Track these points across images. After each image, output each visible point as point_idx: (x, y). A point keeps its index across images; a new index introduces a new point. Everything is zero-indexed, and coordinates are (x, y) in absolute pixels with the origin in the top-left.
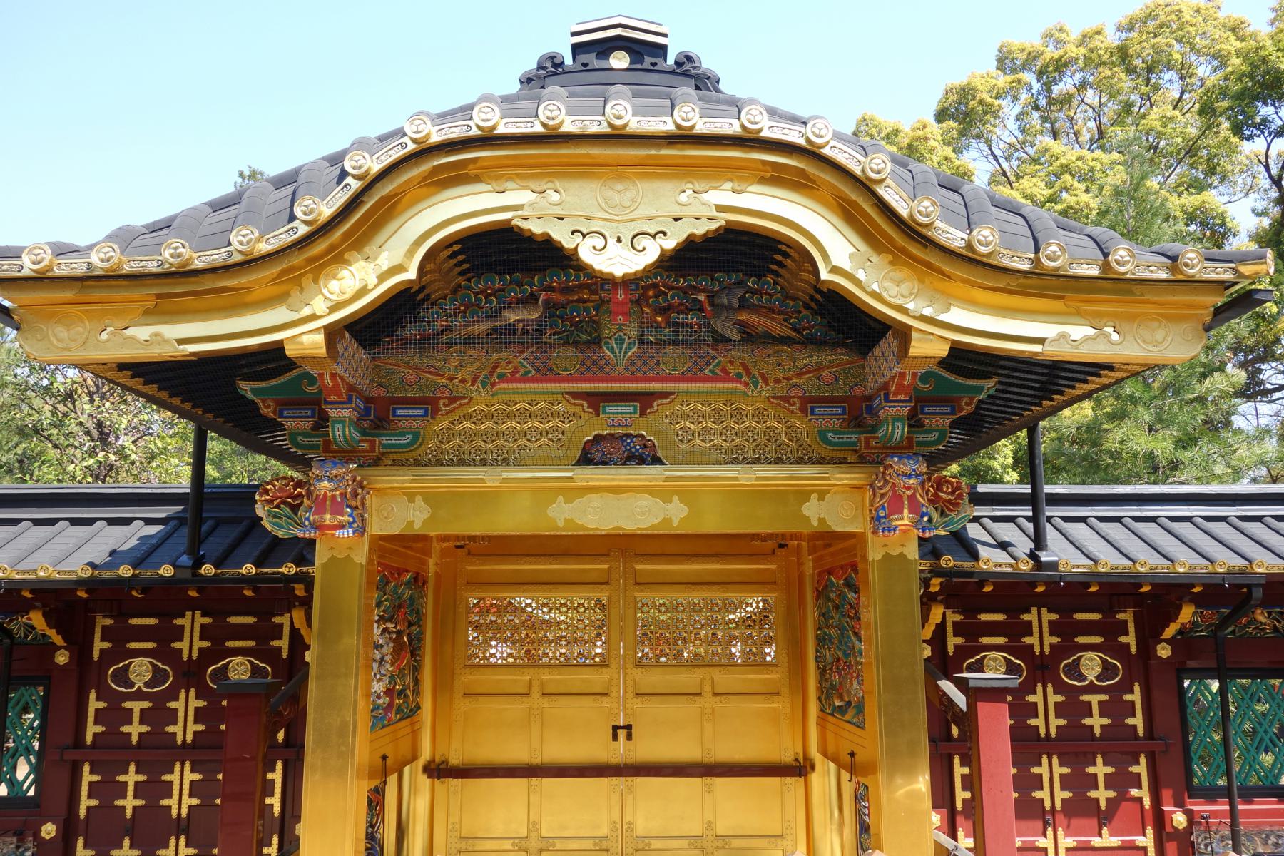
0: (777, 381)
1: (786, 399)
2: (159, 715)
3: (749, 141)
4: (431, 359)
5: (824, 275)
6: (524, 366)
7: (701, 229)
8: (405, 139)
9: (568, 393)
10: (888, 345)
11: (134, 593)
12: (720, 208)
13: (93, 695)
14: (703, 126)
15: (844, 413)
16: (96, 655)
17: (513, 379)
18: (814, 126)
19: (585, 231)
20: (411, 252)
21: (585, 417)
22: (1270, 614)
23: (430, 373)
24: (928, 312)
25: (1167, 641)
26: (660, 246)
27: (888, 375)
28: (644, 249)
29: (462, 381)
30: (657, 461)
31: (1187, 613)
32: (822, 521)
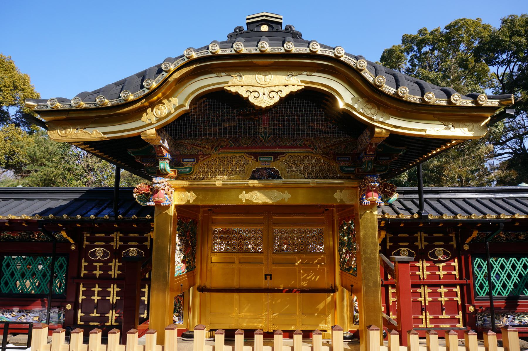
0: (324, 148)
1: (328, 155)
2: (106, 268)
3: (313, 55)
6: (231, 143)
7: (295, 89)
8: (184, 57)
9: (247, 153)
10: (367, 133)
11: (96, 225)
12: (302, 82)
13: (83, 260)
14: (294, 50)
15: (349, 160)
16: (84, 247)
18: (337, 50)
19: (251, 91)
20: (186, 99)
22: (505, 234)
23: (195, 146)
24: (381, 120)
25: (467, 244)
26: (280, 96)
27: (366, 144)
28: (273, 97)
29: (208, 149)
30: (279, 178)
31: (475, 234)
32: (341, 200)
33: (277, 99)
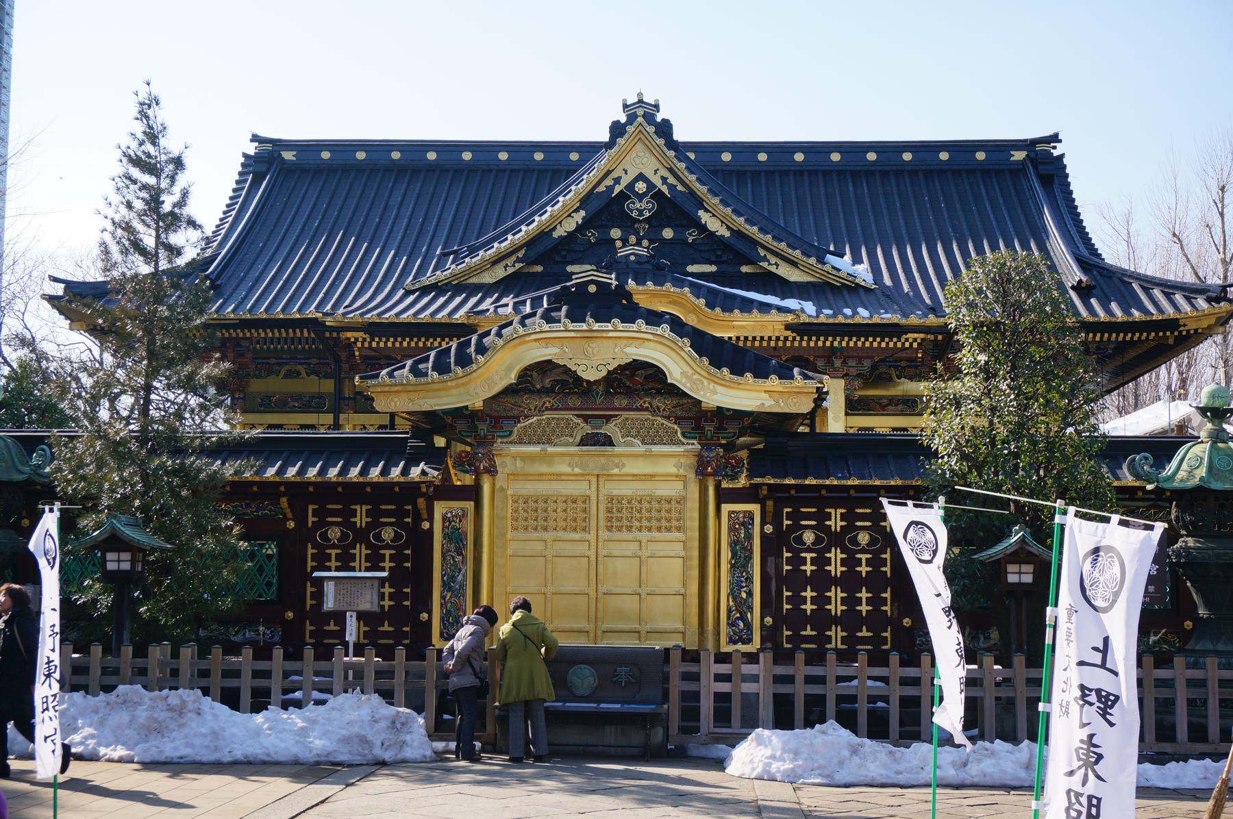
4: (518, 400)
5: (669, 381)
17: (552, 409)
21: (582, 425)
33: (604, 373)
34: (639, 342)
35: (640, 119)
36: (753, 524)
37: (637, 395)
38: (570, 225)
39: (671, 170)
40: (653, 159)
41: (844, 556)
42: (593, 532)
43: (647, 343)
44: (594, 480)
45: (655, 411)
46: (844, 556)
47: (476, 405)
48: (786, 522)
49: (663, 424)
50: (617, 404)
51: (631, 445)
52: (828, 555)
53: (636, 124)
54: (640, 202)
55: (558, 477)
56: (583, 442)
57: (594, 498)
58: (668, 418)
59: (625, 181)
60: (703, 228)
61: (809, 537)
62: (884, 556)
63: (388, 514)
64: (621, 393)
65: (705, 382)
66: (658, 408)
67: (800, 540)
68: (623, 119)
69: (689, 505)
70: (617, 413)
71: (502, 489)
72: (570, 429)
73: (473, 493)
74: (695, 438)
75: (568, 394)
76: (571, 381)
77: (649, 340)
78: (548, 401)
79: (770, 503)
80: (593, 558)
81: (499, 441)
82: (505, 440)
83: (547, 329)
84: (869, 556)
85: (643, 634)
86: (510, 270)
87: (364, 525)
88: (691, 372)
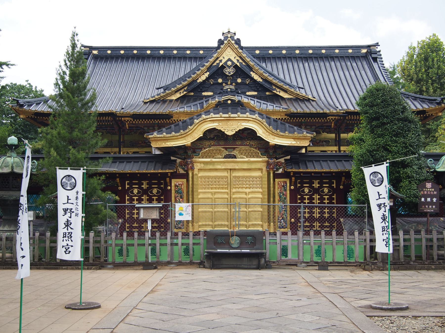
4: (202, 142)
17: (214, 145)
33: (234, 132)
34: (246, 122)
35: (229, 39)
36: (286, 186)
37: (245, 140)
38: (203, 78)
39: (240, 57)
40: (234, 53)
41: (319, 197)
42: (229, 189)
43: (250, 122)
44: (229, 171)
45: (251, 146)
46: (319, 197)
47: (188, 144)
48: (299, 185)
49: (254, 150)
50: (237, 143)
51: (243, 158)
52: (313, 197)
53: (228, 40)
54: (229, 69)
55: (216, 170)
56: (225, 157)
57: (229, 177)
58: (256, 148)
59: (224, 61)
60: (252, 79)
61: (306, 190)
62: (333, 197)
63: (155, 184)
64: (239, 139)
65: (271, 135)
66: (252, 144)
67: (303, 191)
68: (223, 39)
69: (264, 179)
70: (237, 147)
71: (196, 174)
72: (220, 152)
73: (186, 176)
74: (265, 155)
75: (220, 140)
76: (220, 135)
77: (250, 120)
78: (212, 142)
79: (293, 178)
80: (229, 199)
81: (195, 157)
82: (197, 157)
83: (214, 117)
84: (328, 197)
85: (248, 226)
86: (182, 94)
87: (146, 188)
88: (265, 132)
